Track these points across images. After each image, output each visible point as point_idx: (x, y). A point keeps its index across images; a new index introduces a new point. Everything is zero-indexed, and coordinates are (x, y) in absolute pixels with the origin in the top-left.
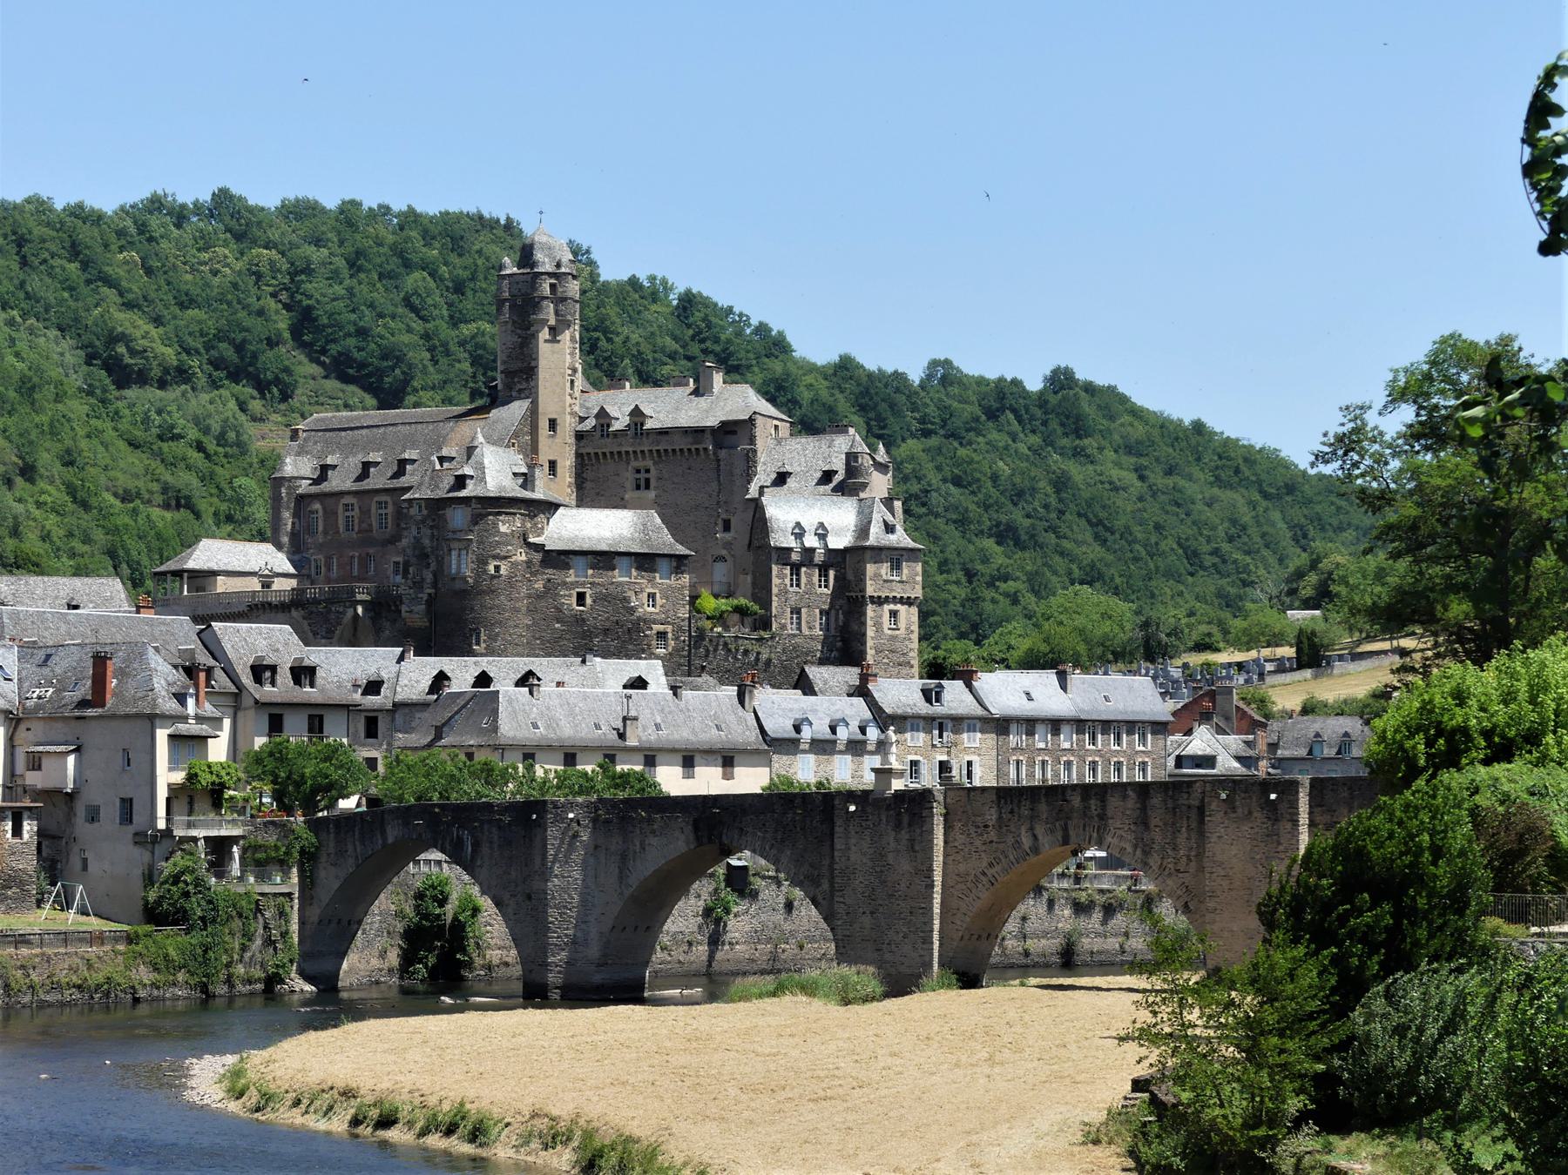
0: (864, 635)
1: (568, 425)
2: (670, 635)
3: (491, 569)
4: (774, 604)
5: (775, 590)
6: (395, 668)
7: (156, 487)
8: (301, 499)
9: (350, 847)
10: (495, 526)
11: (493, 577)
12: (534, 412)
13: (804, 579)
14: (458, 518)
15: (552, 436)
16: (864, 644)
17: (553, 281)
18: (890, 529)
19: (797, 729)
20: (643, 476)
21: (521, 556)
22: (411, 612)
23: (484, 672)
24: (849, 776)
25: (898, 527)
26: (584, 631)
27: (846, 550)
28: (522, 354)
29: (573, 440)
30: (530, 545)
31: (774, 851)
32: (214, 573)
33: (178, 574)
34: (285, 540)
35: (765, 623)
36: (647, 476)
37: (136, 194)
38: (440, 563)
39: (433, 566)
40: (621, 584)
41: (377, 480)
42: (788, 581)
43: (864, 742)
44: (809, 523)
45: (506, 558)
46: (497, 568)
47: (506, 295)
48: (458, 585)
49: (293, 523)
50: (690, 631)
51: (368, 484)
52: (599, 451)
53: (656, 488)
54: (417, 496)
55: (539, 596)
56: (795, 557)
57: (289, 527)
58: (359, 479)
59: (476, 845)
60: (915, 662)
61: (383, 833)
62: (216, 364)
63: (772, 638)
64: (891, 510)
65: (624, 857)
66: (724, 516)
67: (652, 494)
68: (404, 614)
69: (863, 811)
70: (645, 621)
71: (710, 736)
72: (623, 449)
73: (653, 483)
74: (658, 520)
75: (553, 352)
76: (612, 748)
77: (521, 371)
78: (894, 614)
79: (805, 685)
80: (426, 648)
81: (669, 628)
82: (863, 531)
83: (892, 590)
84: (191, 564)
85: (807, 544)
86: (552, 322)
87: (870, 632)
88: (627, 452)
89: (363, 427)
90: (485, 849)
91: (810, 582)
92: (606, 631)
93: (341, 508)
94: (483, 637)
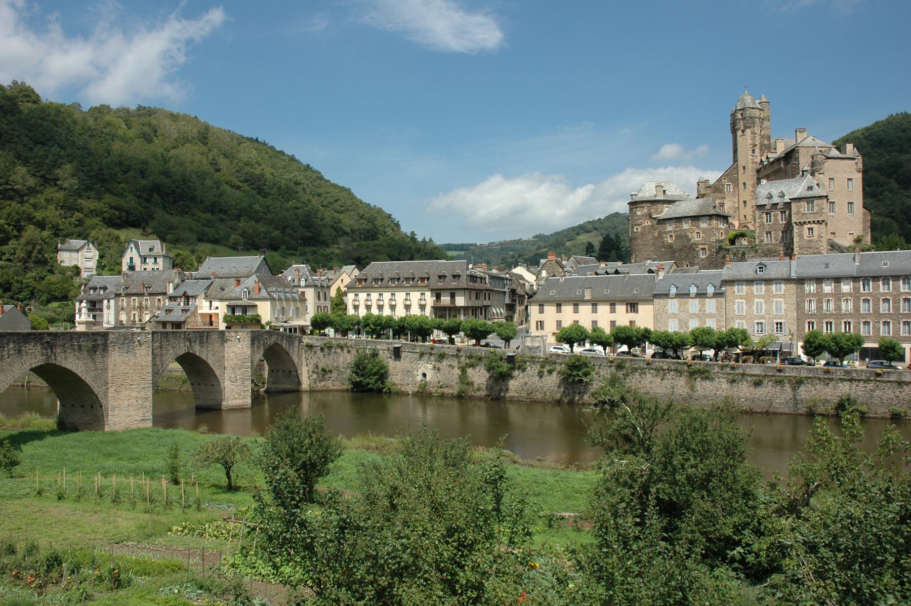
13: (772, 218)
30: (652, 218)
40: (685, 230)
42: (765, 220)
44: (775, 192)
55: (657, 238)
81: (706, 247)
86: (742, 128)
87: (796, 240)
91: (776, 219)
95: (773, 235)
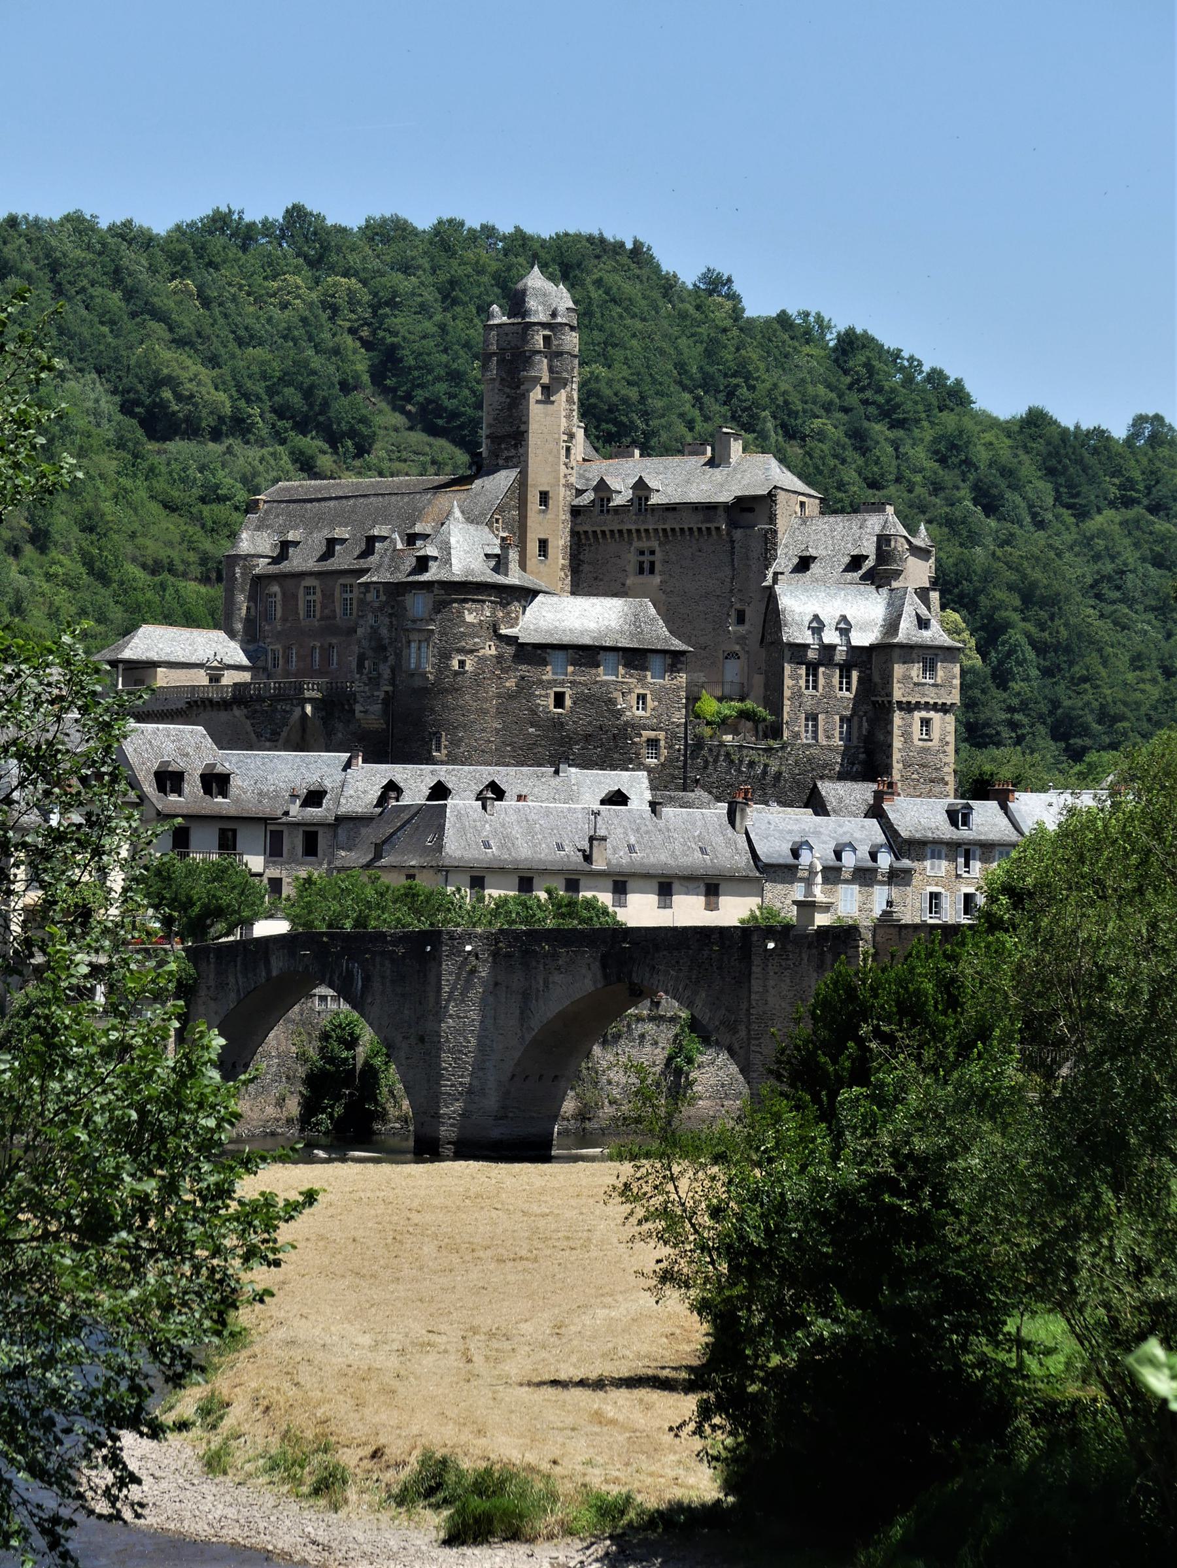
0: (890, 746)
1: (562, 499)
2: (662, 743)
3: (455, 664)
4: (786, 709)
5: (787, 693)
6: (339, 776)
7: (192, 557)
8: (259, 581)
9: (232, 980)
10: (460, 614)
11: (456, 673)
12: (522, 483)
13: (821, 681)
14: (418, 605)
15: (543, 511)
16: (890, 756)
17: (547, 333)
18: (923, 624)
19: (795, 853)
20: (646, 558)
21: (490, 650)
22: (365, 712)
23: (439, 782)
24: (856, 909)
25: (933, 622)
26: (563, 738)
27: (872, 648)
28: (510, 416)
29: (568, 516)
31: (688, 993)
32: (154, 665)
33: (114, 663)
34: (239, 626)
35: (775, 731)
36: (651, 558)
37: (196, 211)
38: (399, 656)
39: (391, 659)
40: (606, 683)
41: (343, 560)
42: (802, 683)
43: (875, 870)
45: (471, 651)
46: (462, 663)
47: (494, 348)
48: (417, 683)
49: (248, 608)
50: (686, 738)
51: (333, 564)
52: (598, 529)
53: (662, 573)
54: (374, 579)
55: (511, 696)
56: (812, 655)
57: (244, 612)
58: (323, 558)
59: (367, 979)
60: (950, 779)
61: (267, 963)
62: (281, 412)
63: (783, 748)
64: (926, 602)
65: (526, 996)
66: (738, 606)
67: (657, 580)
68: (358, 715)
69: (784, 948)
70: (633, 726)
71: (693, 860)
72: (625, 527)
73: (658, 567)
74: (653, 611)
75: (546, 415)
76: (575, 872)
77: (509, 436)
78: (926, 722)
79: (817, 804)
80: (376, 755)
81: (662, 735)
82: (892, 626)
83: (924, 695)
84: (127, 654)
85: (826, 641)
86: (545, 380)
87: (897, 743)
88: (629, 531)
89: (331, 499)
90: (376, 985)
91: (829, 685)
92: (588, 738)
93: (301, 592)
94: (444, 742)
95: (821, 723)
